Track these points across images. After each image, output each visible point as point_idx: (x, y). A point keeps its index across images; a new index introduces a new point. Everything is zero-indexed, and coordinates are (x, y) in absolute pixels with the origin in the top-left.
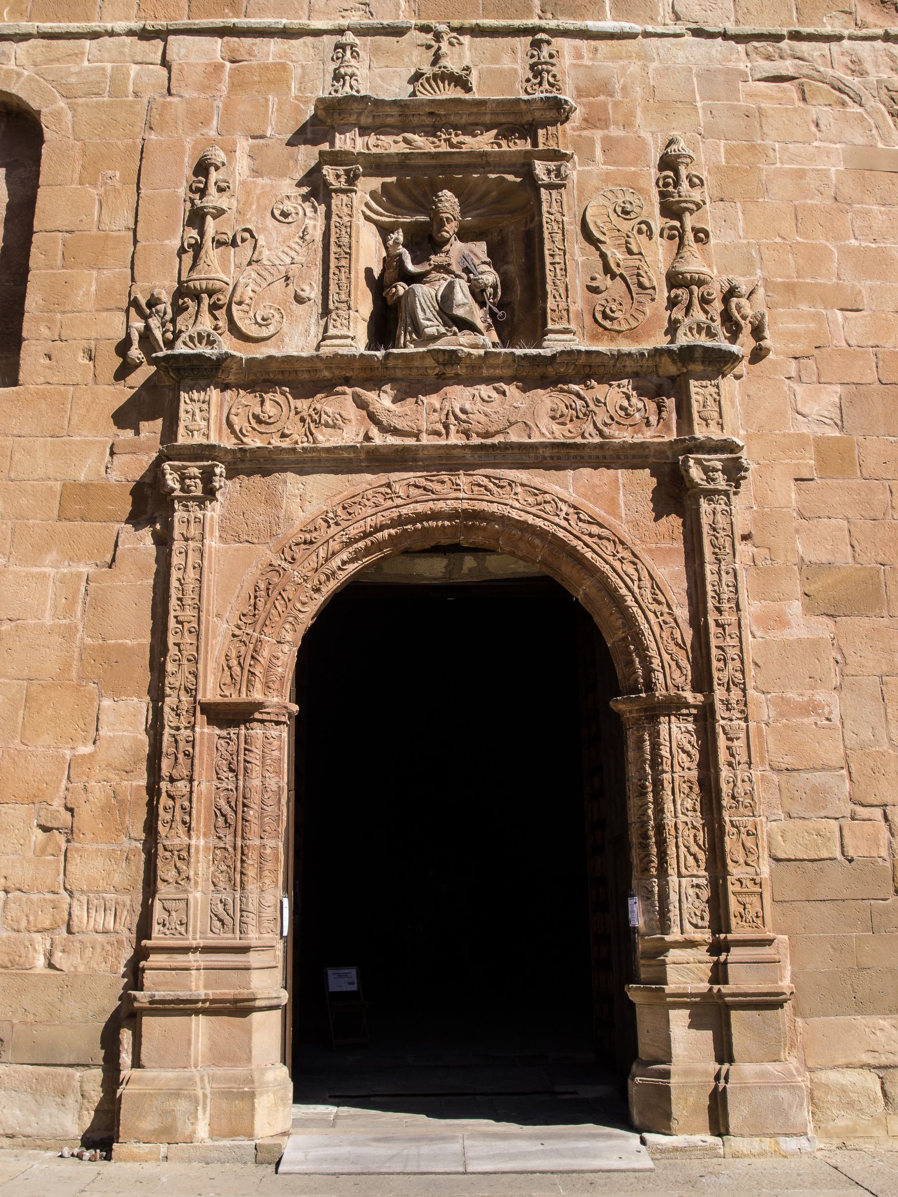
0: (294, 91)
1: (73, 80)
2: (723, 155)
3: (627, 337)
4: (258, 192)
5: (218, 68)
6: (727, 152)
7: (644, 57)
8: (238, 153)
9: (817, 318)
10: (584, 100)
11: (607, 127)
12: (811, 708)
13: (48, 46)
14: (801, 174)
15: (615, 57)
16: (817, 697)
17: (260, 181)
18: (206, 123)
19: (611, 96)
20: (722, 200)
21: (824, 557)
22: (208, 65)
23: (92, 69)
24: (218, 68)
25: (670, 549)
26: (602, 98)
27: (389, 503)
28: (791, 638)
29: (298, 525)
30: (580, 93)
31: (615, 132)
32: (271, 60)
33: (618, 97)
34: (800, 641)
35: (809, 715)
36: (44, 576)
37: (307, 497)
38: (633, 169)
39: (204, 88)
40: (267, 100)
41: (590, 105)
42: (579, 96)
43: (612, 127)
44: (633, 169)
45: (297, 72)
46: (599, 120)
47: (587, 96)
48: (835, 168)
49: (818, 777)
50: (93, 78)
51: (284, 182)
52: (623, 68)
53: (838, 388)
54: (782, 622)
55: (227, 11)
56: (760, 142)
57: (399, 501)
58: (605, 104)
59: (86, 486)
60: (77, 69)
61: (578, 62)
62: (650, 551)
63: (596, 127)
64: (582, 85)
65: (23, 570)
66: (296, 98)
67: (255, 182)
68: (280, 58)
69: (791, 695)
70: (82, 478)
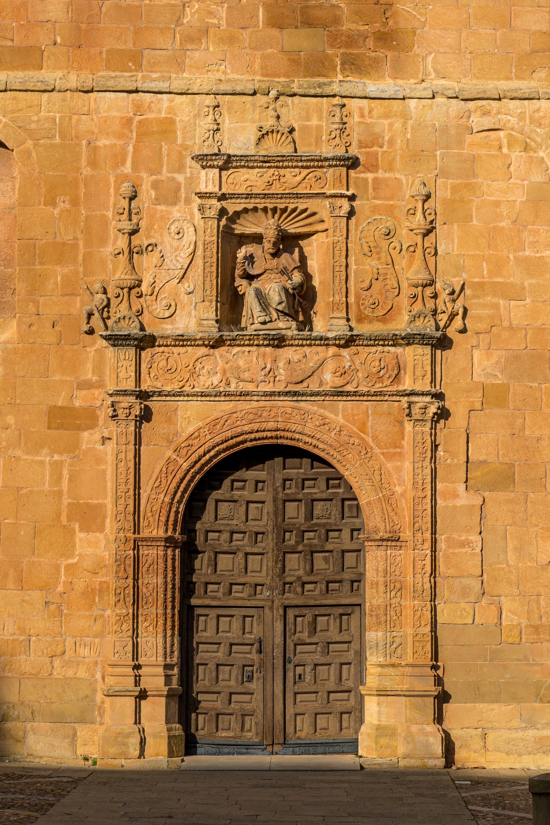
0: (179, 142)
1: (33, 126)
2: (449, 191)
3: (378, 321)
4: (158, 216)
5: (129, 121)
6: (453, 188)
7: (405, 116)
8: (144, 186)
9: (496, 306)
10: (364, 150)
11: (377, 171)
12: (463, 544)
13: (14, 99)
14: (497, 204)
15: (387, 116)
16: (471, 538)
17: (159, 208)
18: (123, 163)
19: (381, 147)
20: (445, 224)
21: (482, 458)
22: (122, 118)
23: (47, 119)
24: (129, 121)
25: (395, 453)
26: (375, 148)
27: (238, 423)
28: (459, 505)
29: (185, 436)
30: (361, 145)
31: (380, 174)
32: (163, 115)
33: (385, 148)
34: (462, 506)
35: (465, 547)
36: (42, 463)
37: (191, 419)
38: (391, 203)
39: (120, 136)
40: (161, 147)
41: (367, 153)
42: (360, 147)
43: (380, 171)
44: (391, 203)
45: (179, 126)
46: (372, 166)
47: (365, 147)
48: (520, 197)
49: (466, 581)
50: (46, 125)
51: (174, 209)
52: (391, 125)
53: (504, 352)
54: (455, 495)
55: (130, 64)
56: (474, 180)
57: (244, 422)
58: (377, 154)
59: (61, 408)
60: (35, 118)
61: (362, 120)
62: (383, 454)
63: (370, 171)
64: (362, 138)
65: (30, 457)
66: (181, 145)
67: (155, 209)
68: (170, 113)
69: (455, 536)
70: (60, 404)
